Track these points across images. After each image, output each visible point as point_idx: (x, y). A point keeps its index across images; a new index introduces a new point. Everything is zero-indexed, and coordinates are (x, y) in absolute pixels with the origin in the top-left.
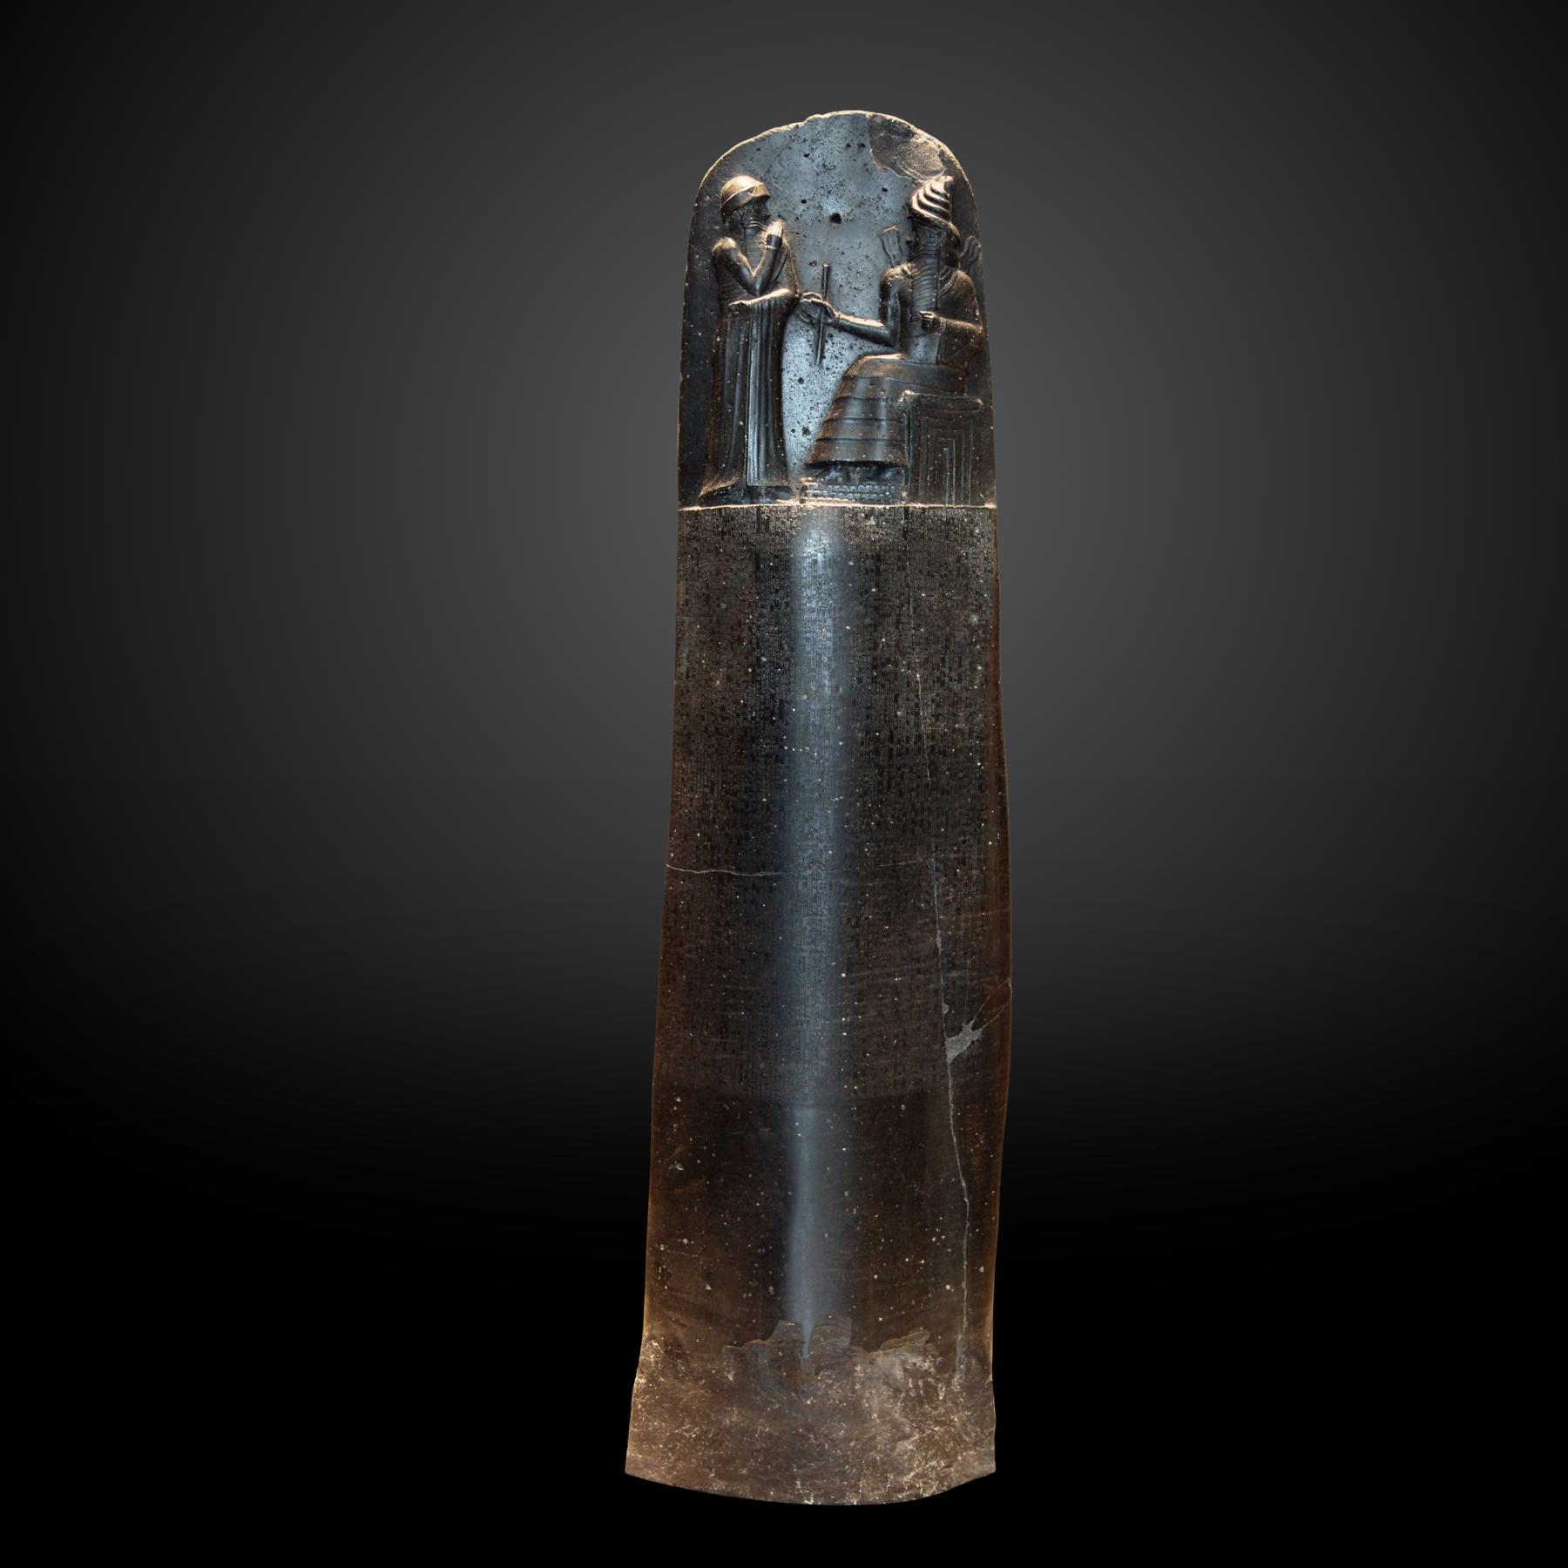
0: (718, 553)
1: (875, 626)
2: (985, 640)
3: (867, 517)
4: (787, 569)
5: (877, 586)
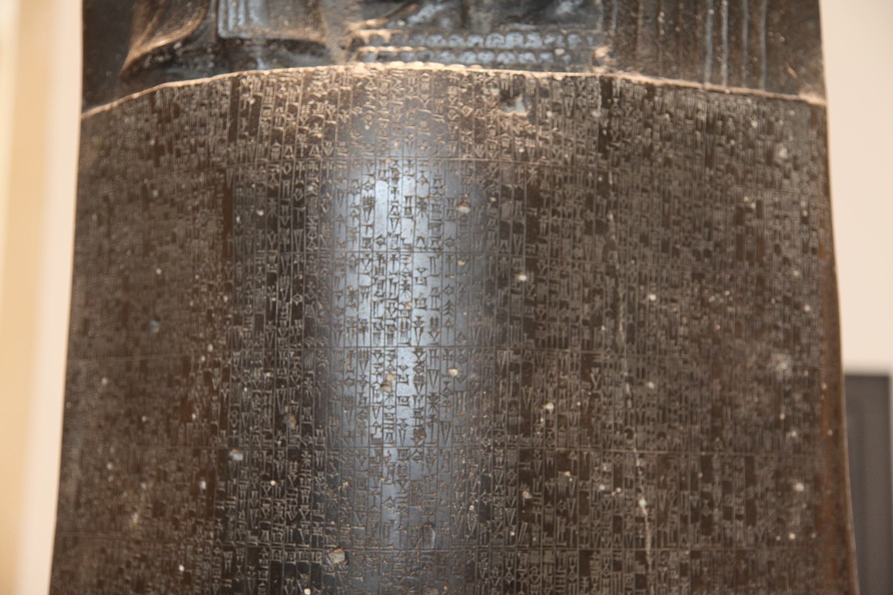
0: (147, 199)
1: (527, 370)
2: (811, 418)
3: (507, 98)
4: (299, 222)
5: (531, 265)
